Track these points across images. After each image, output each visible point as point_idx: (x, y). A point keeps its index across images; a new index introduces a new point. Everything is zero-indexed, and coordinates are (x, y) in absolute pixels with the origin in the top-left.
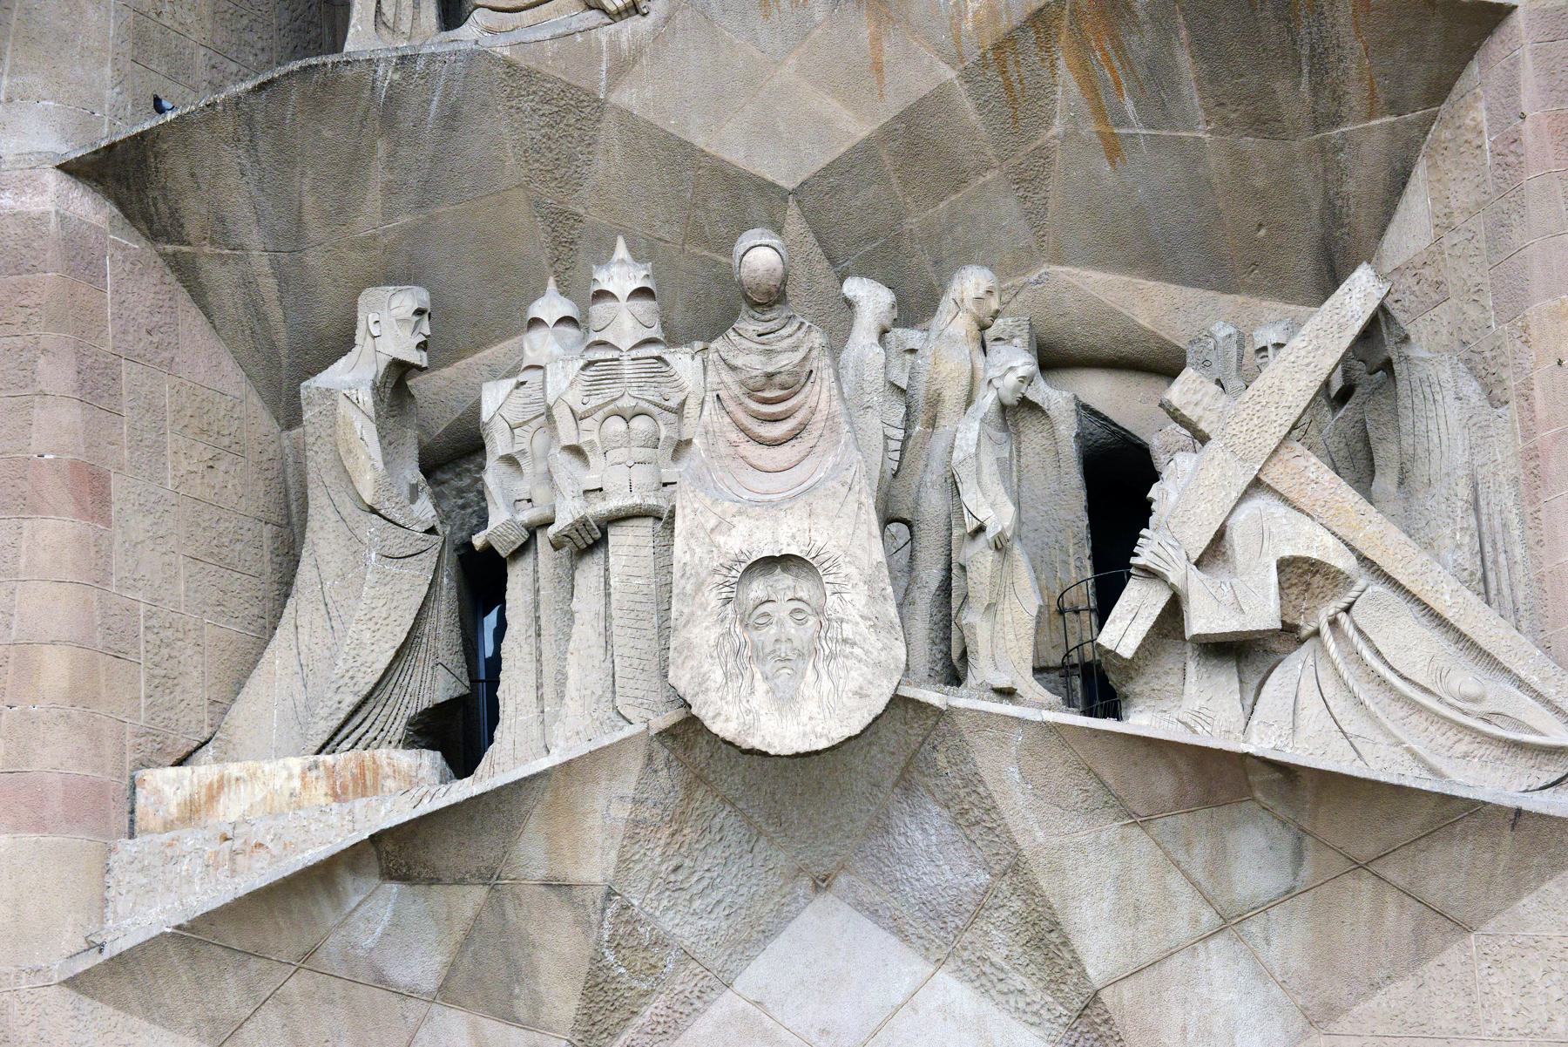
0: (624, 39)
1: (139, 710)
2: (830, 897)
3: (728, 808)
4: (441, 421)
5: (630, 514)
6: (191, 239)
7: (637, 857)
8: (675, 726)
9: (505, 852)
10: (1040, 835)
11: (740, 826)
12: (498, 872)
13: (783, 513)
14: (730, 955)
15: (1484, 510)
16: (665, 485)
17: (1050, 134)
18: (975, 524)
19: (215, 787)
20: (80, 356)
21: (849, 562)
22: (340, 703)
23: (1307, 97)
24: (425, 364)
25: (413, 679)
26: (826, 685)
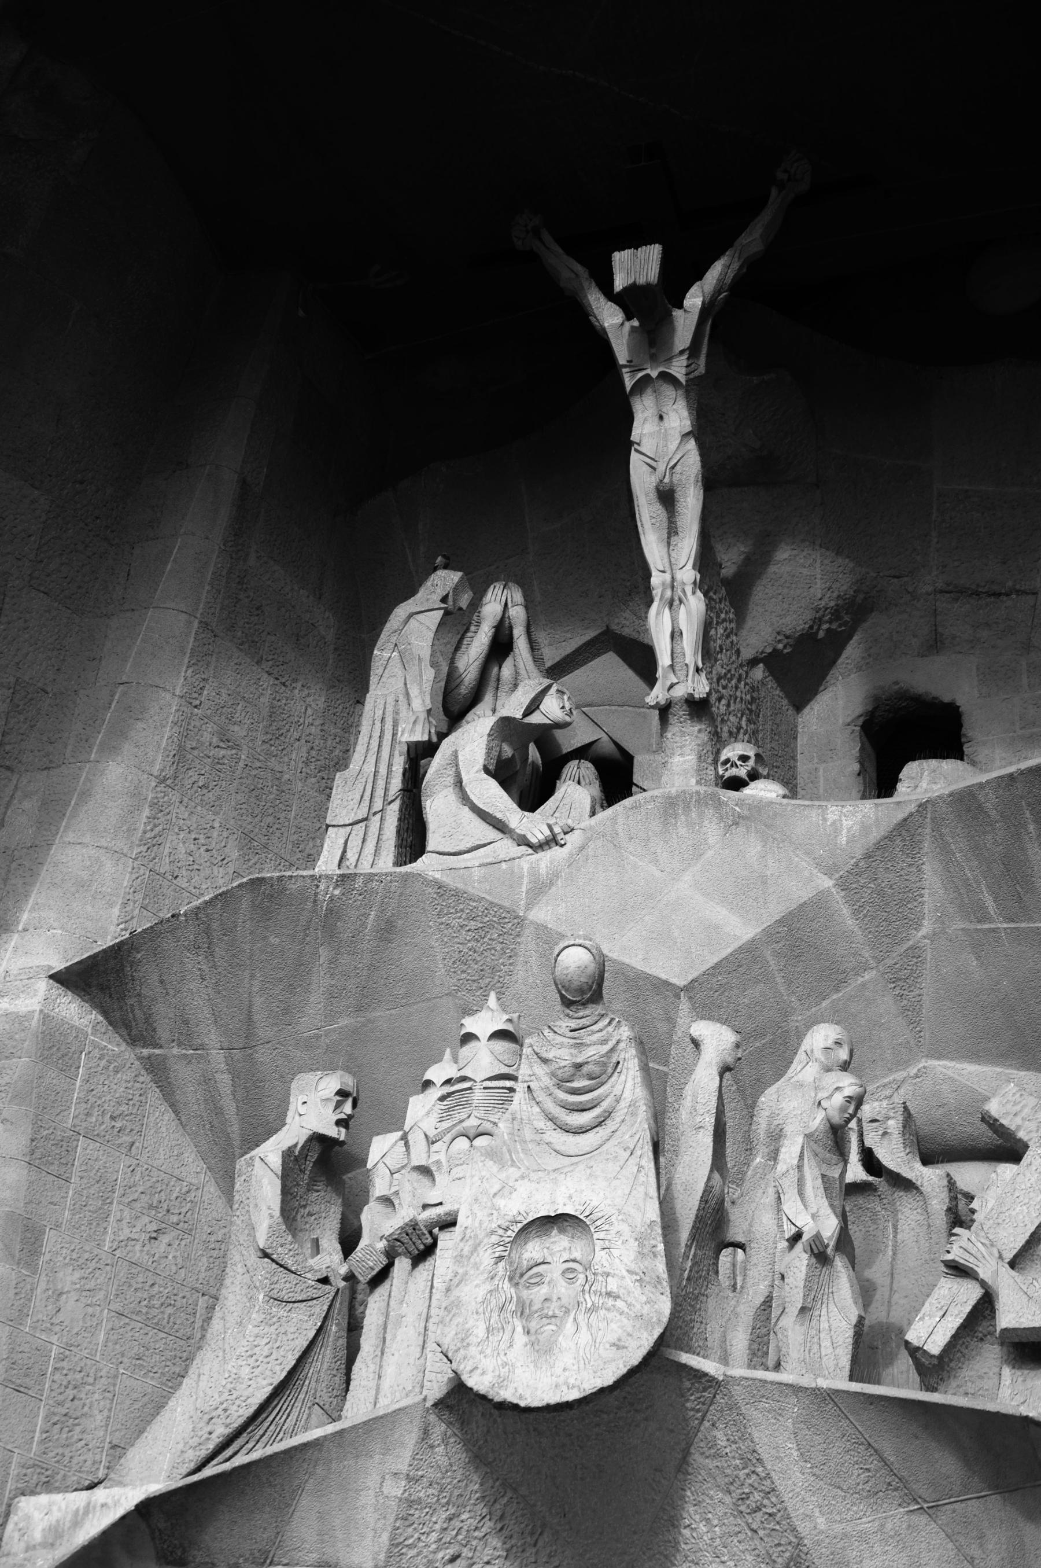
0: (543, 865)
1: (32, 1443)
3: (509, 1494)
6: (162, 1042)
7: (410, 1541)
9: (278, 1533)
10: (821, 1521)
11: (523, 1515)
12: (271, 1555)
13: (563, 1176)
17: (920, 934)
18: (794, 1230)
19: (81, 1513)
20: (37, 1125)
21: (622, 1220)
22: (210, 1433)
24: (342, 1138)
25: (290, 1418)
26: (584, 1336)
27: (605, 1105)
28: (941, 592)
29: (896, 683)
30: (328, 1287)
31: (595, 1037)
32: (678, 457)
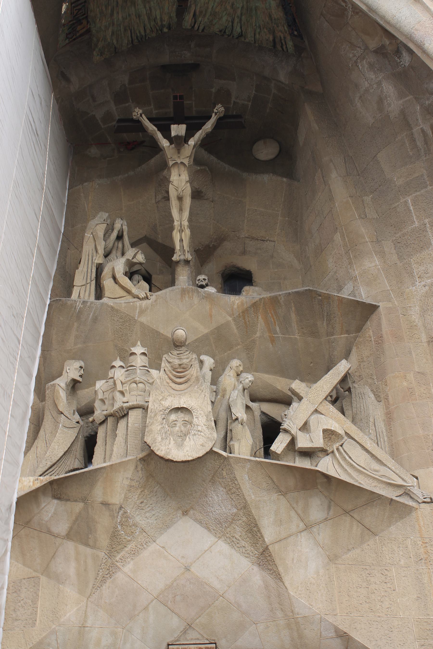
0: (143, 305)
2: (187, 517)
4: (84, 403)
5: (136, 407)
7: (130, 497)
8: (145, 456)
10: (253, 497)
13: (182, 396)
14: (156, 532)
15: (377, 426)
16: (146, 402)
17: (256, 336)
18: (235, 417)
23: (325, 326)
24: (81, 380)
26: (192, 443)
27: (187, 377)
28: (247, 238)
29: (232, 263)
30: (78, 424)
31: (185, 357)
32: (184, 188)
